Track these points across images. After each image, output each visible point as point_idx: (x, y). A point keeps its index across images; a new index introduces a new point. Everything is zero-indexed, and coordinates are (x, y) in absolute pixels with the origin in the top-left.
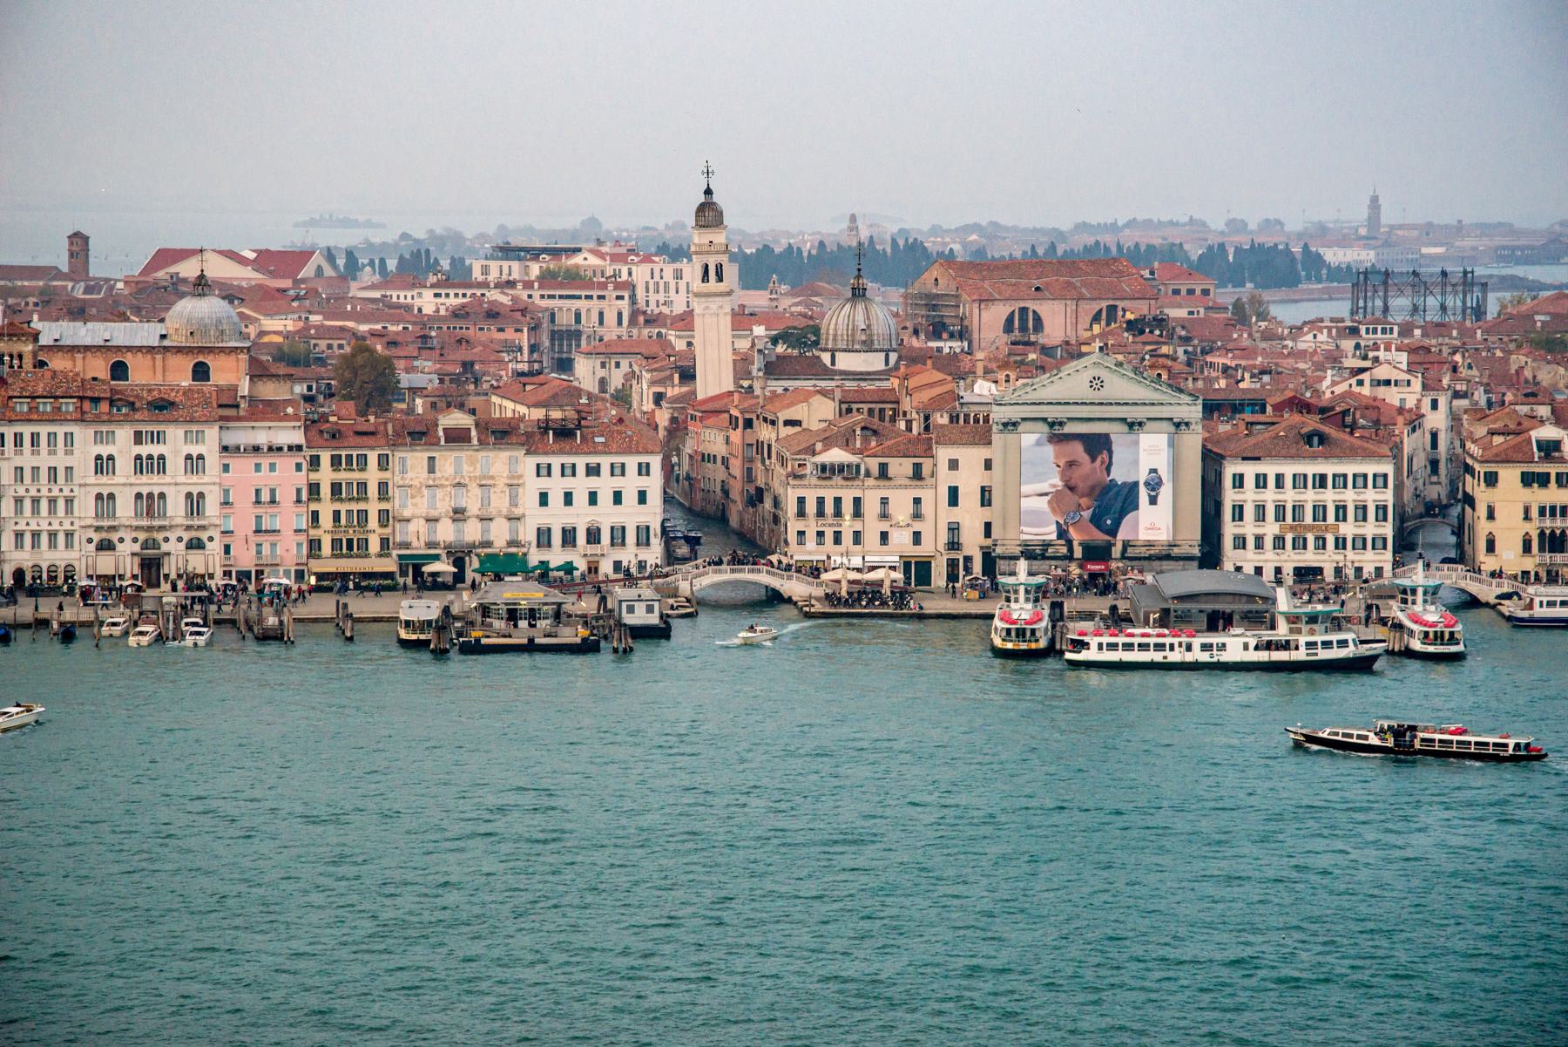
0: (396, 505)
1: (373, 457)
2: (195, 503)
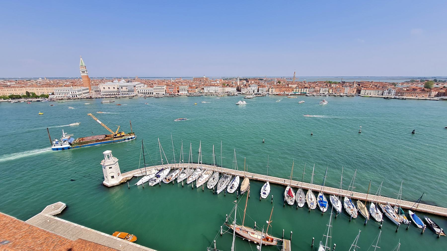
0: (225, 90)
2: (218, 89)
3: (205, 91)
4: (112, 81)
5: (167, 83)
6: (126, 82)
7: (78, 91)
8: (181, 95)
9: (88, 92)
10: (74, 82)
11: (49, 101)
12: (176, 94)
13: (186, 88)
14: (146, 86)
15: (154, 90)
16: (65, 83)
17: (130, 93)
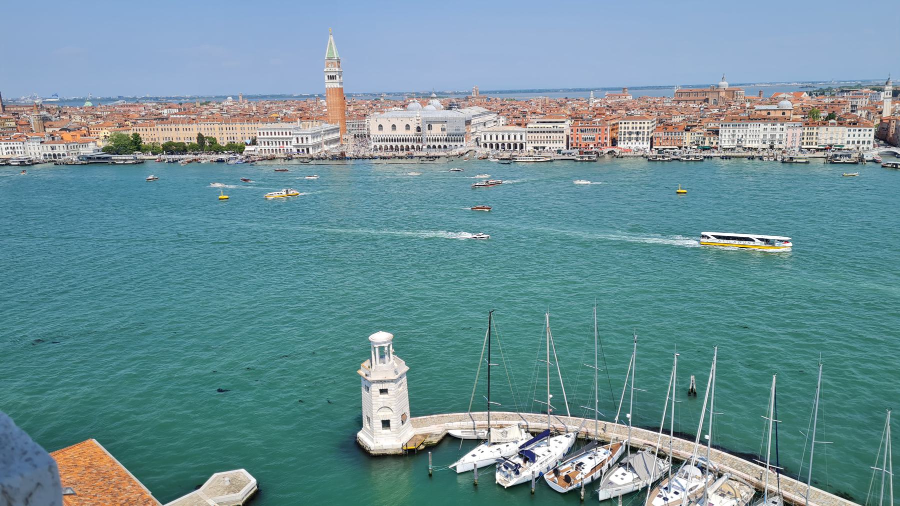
1: (815, 128)
2: (781, 135)
3: (726, 139)
4: (404, 106)
5: (573, 109)
6: (442, 107)
7: (315, 135)
8: (622, 157)
9: (337, 140)
10: (305, 106)
11: (244, 161)
12: (606, 151)
13: (646, 130)
14: (502, 120)
15: (528, 135)
16: (284, 111)
17: (453, 144)
